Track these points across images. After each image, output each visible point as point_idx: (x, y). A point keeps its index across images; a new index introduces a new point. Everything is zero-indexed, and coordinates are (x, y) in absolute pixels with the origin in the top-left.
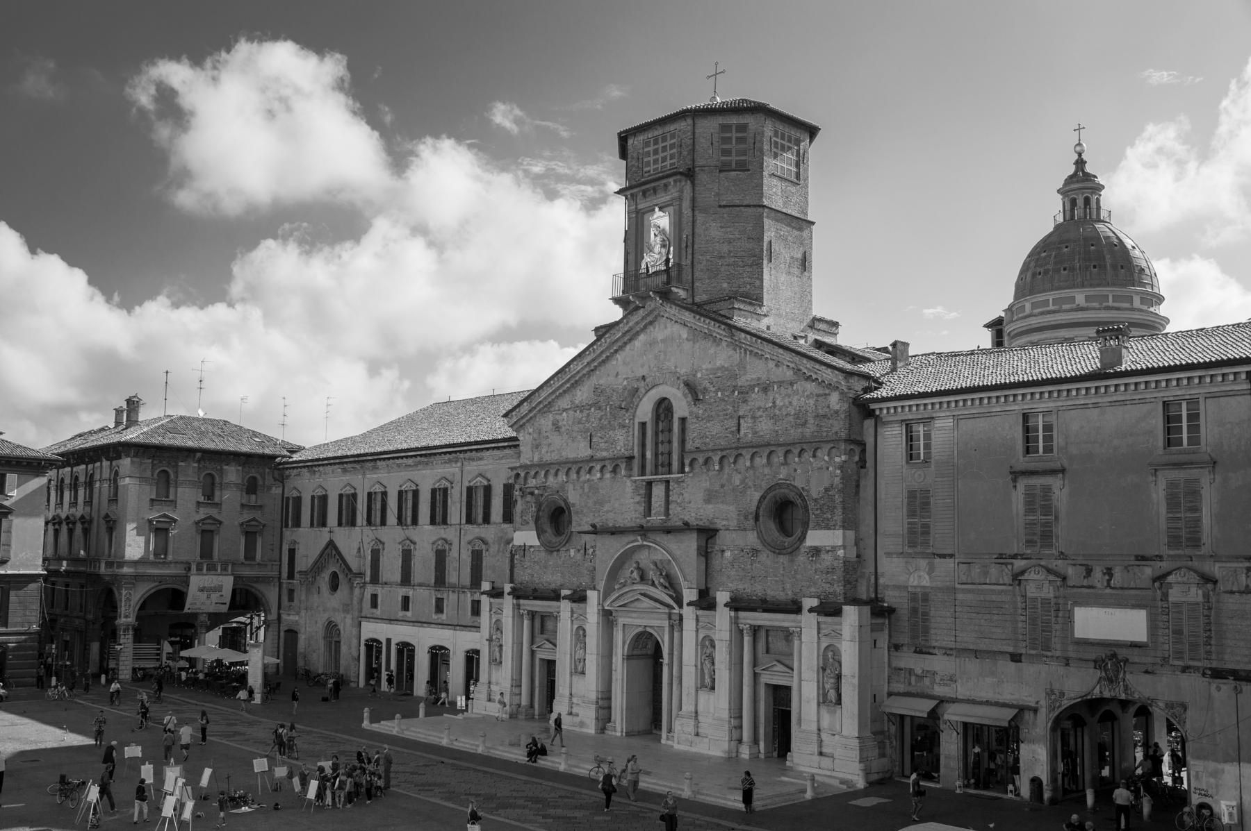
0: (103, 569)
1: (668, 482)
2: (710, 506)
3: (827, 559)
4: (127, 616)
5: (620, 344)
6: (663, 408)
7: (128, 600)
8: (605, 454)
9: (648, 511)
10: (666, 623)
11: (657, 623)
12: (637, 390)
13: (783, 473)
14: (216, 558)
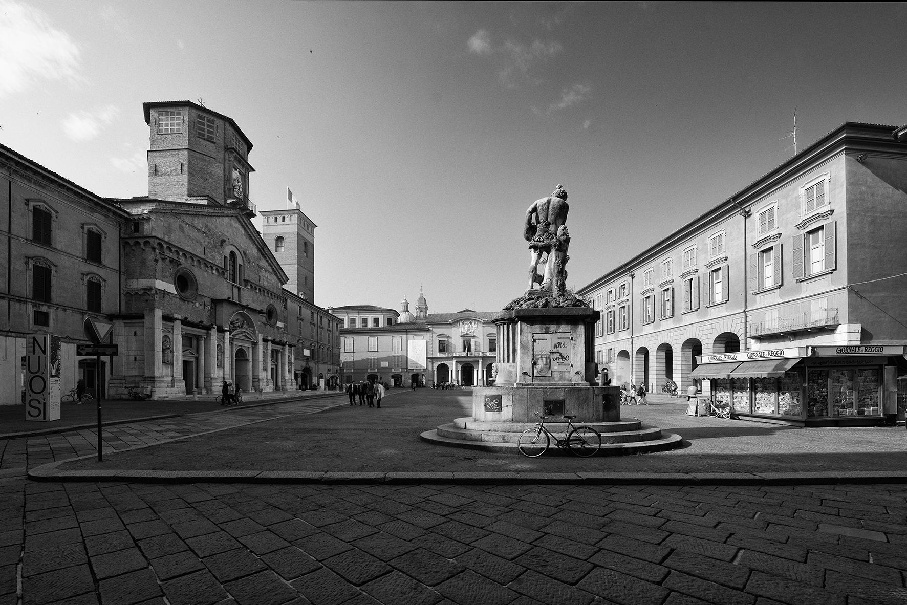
11: (246, 345)
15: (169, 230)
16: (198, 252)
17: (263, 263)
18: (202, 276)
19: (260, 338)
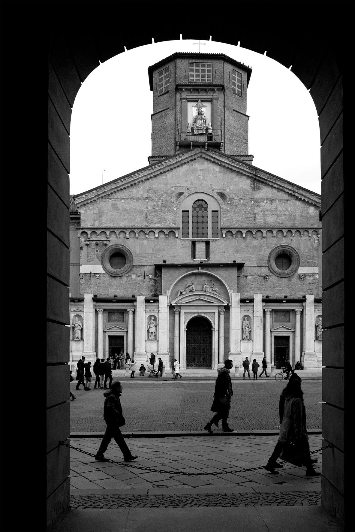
1: (208, 243)
2: (238, 255)
3: (309, 279)
5: (172, 167)
6: (200, 205)
8: (158, 225)
9: (194, 256)
10: (216, 311)
12: (182, 193)
13: (284, 241)
15: (100, 215)
16: (139, 222)
17: (265, 192)
18: (135, 246)
19: (235, 298)
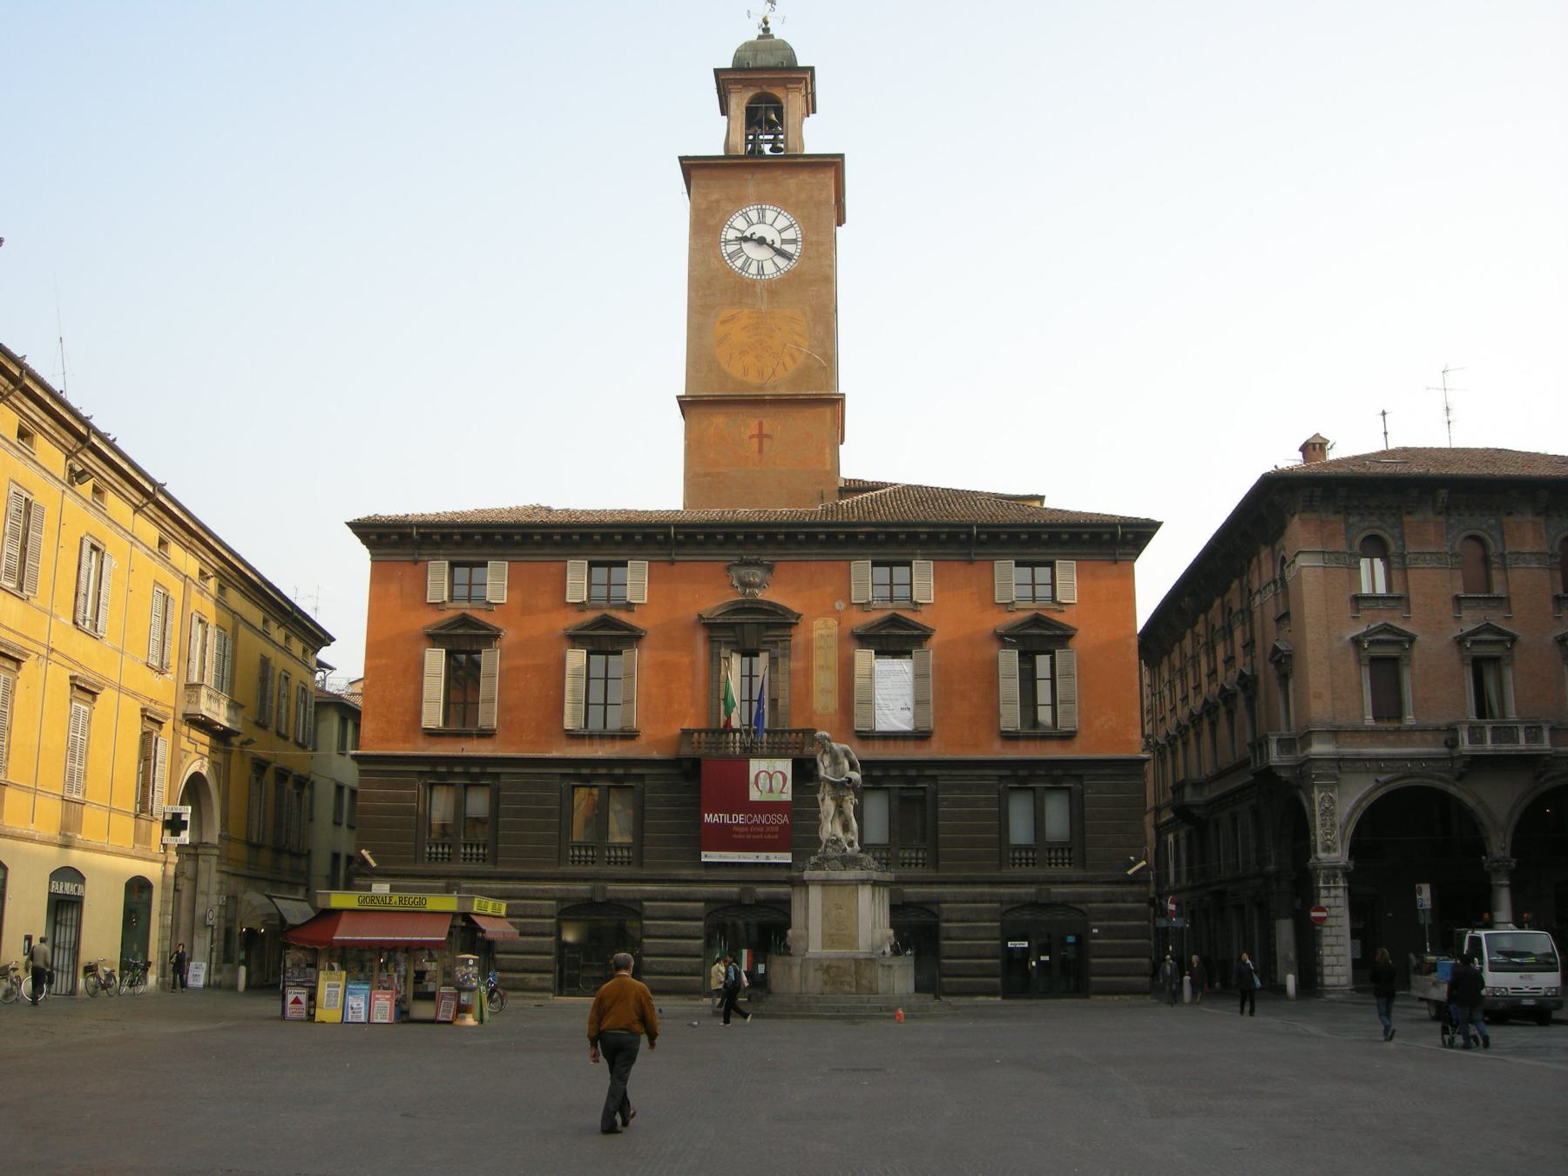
0: (1275, 756)
4: (1331, 848)
7: (1329, 812)
14: (1512, 715)
